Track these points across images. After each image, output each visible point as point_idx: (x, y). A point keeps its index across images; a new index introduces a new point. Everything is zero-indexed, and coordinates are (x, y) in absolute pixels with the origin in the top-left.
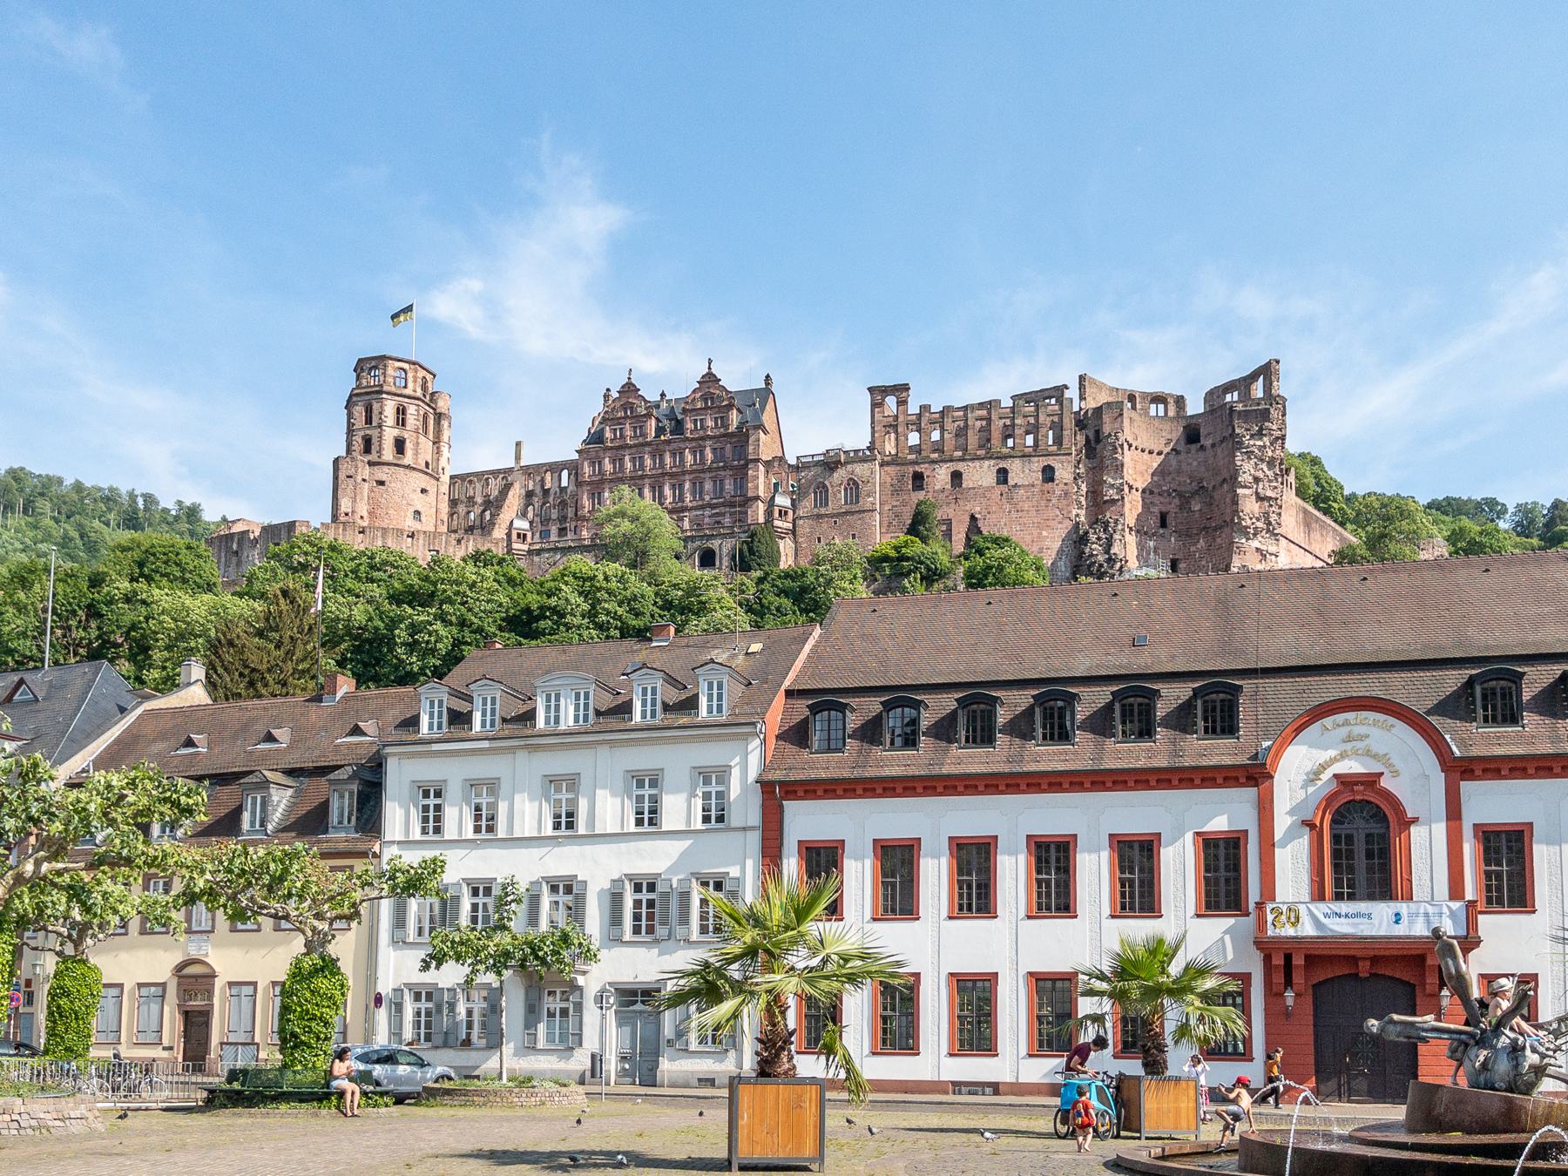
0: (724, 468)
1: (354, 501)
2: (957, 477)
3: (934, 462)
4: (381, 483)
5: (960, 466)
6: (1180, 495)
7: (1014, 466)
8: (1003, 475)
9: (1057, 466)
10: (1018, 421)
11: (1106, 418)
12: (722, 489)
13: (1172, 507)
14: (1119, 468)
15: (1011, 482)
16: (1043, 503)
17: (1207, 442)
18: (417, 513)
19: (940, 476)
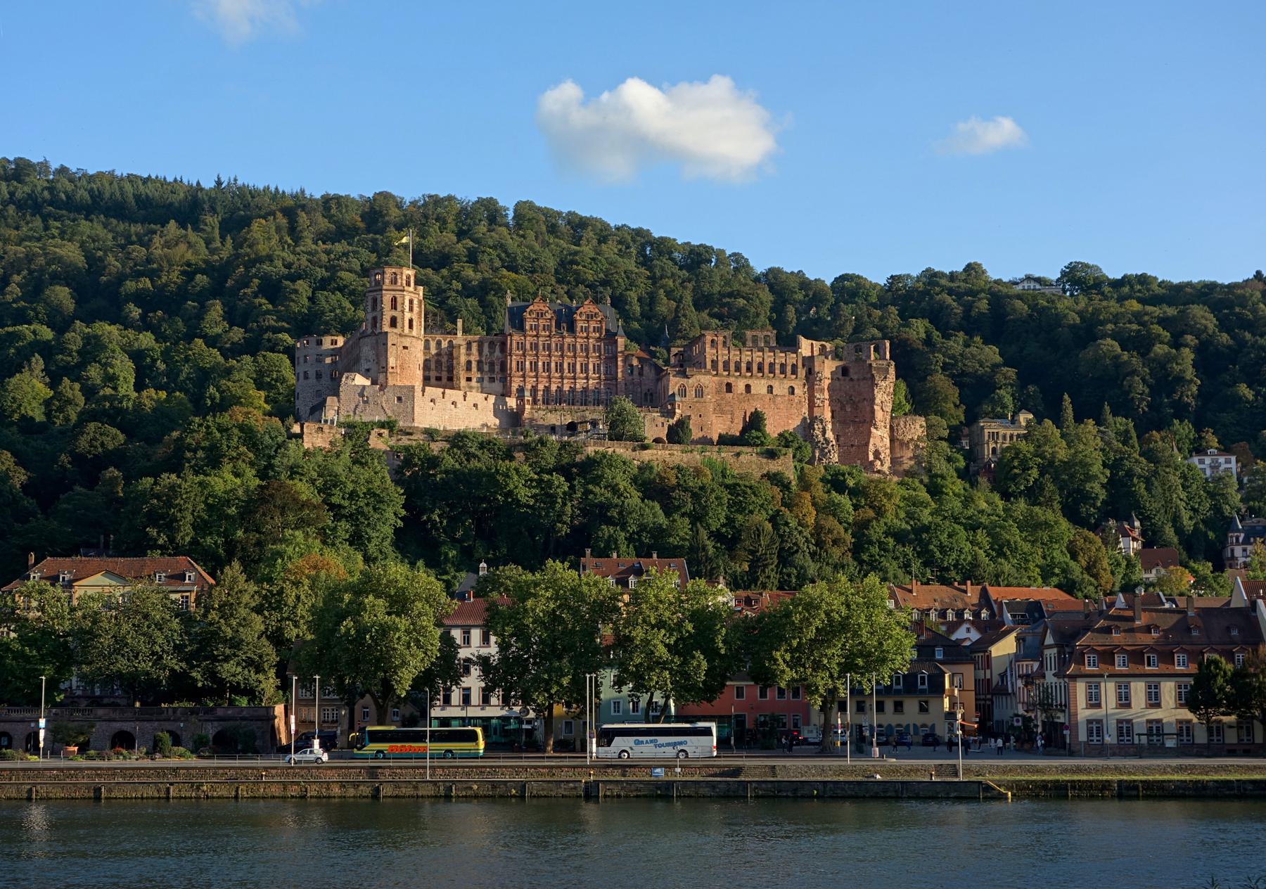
2: (748, 387)
4: (405, 348)
7: (775, 384)
8: (770, 389)
19: (740, 386)
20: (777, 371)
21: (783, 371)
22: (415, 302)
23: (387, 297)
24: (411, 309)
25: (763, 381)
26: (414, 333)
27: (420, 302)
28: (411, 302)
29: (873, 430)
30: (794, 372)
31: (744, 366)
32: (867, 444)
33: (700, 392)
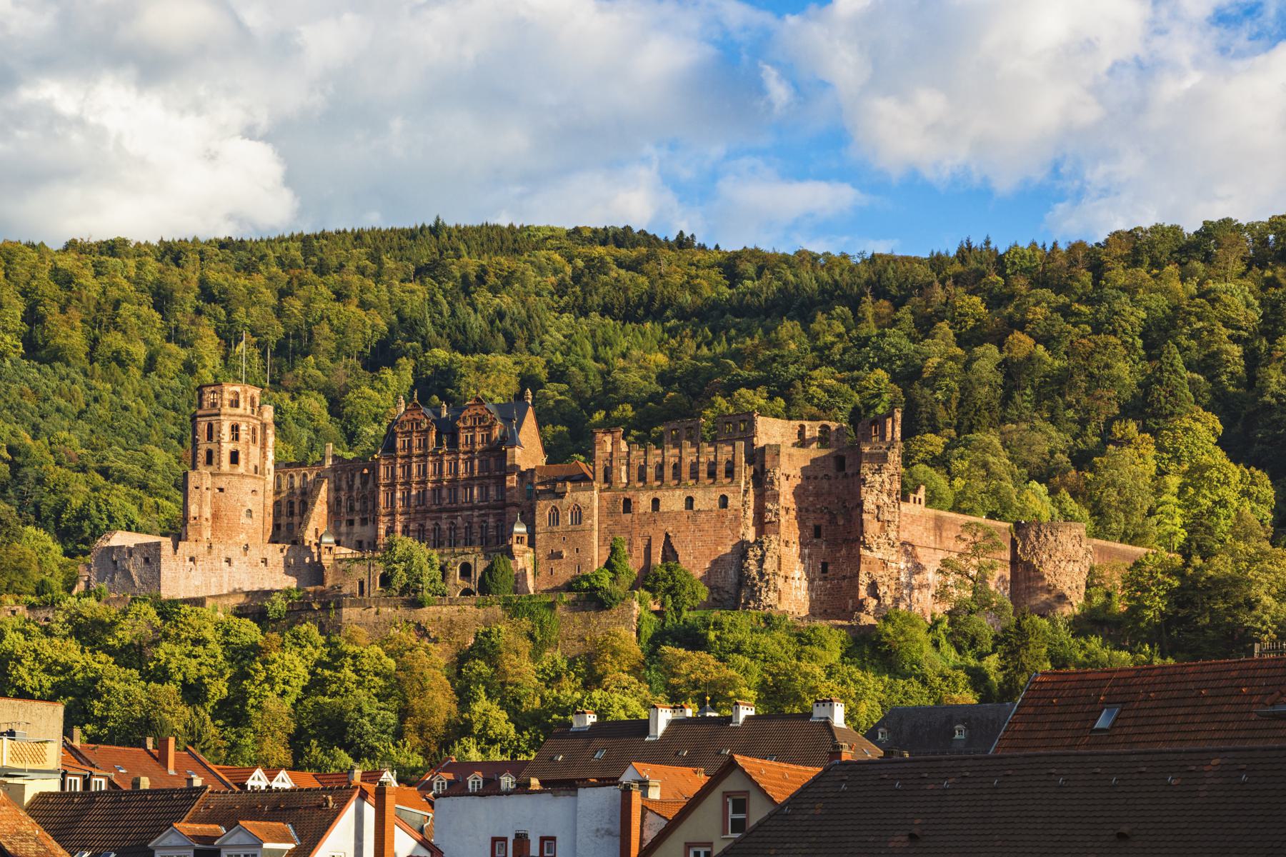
0: (488, 477)
1: (200, 507)
2: (656, 502)
3: (638, 490)
4: (221, 490)
5: (659, 494)
6: (830, 513)
7: (698, 495)
8: (690, 502)
9: (730, 495)
10: (701, 460)
11: (768, 458)
12: (487, 494)
13: (824, 522)
14: (776, 497)
15: (695, 508)
16: (719, 525)
17: (849, 471)
18: (250, 511)
19: (643, 502)
20: (703, 475)
21: (712, 474)
22: (243, 427)
23: (203, 426)
24: (236, 438)
25: (678, 492)
26: (241, 468)
27: (264, 426)
28: (235, 428)
29: (863, 552)
30: (730, 472)
31: (651, 472)
32: (857, 575)
33: (579, 514)
